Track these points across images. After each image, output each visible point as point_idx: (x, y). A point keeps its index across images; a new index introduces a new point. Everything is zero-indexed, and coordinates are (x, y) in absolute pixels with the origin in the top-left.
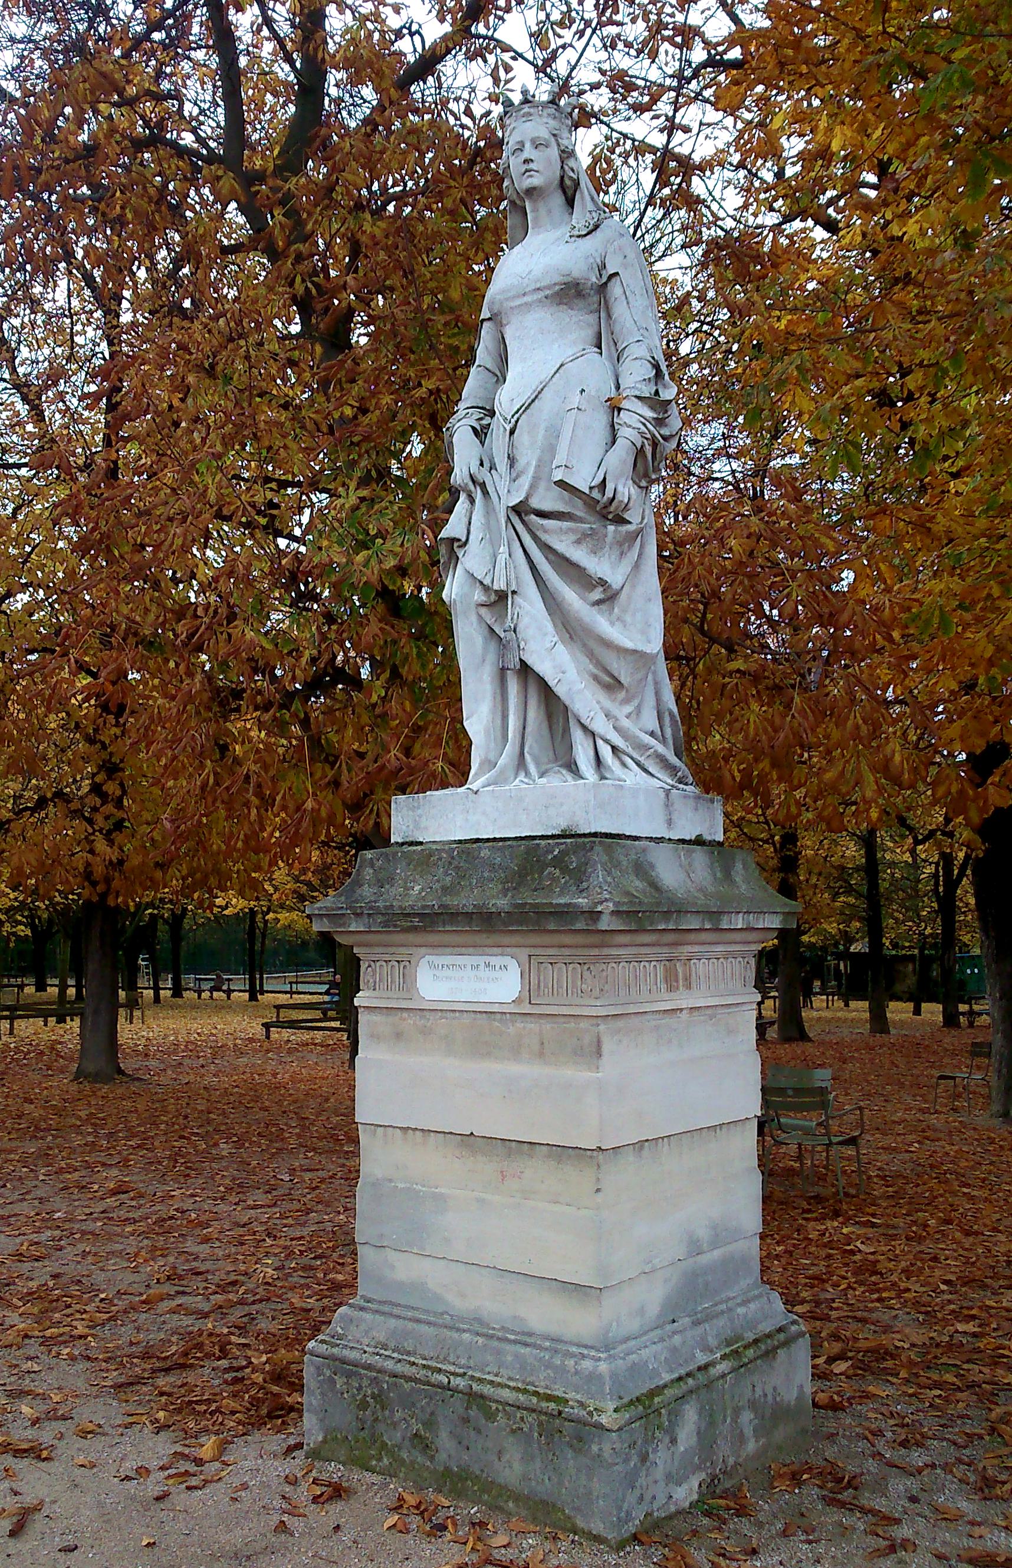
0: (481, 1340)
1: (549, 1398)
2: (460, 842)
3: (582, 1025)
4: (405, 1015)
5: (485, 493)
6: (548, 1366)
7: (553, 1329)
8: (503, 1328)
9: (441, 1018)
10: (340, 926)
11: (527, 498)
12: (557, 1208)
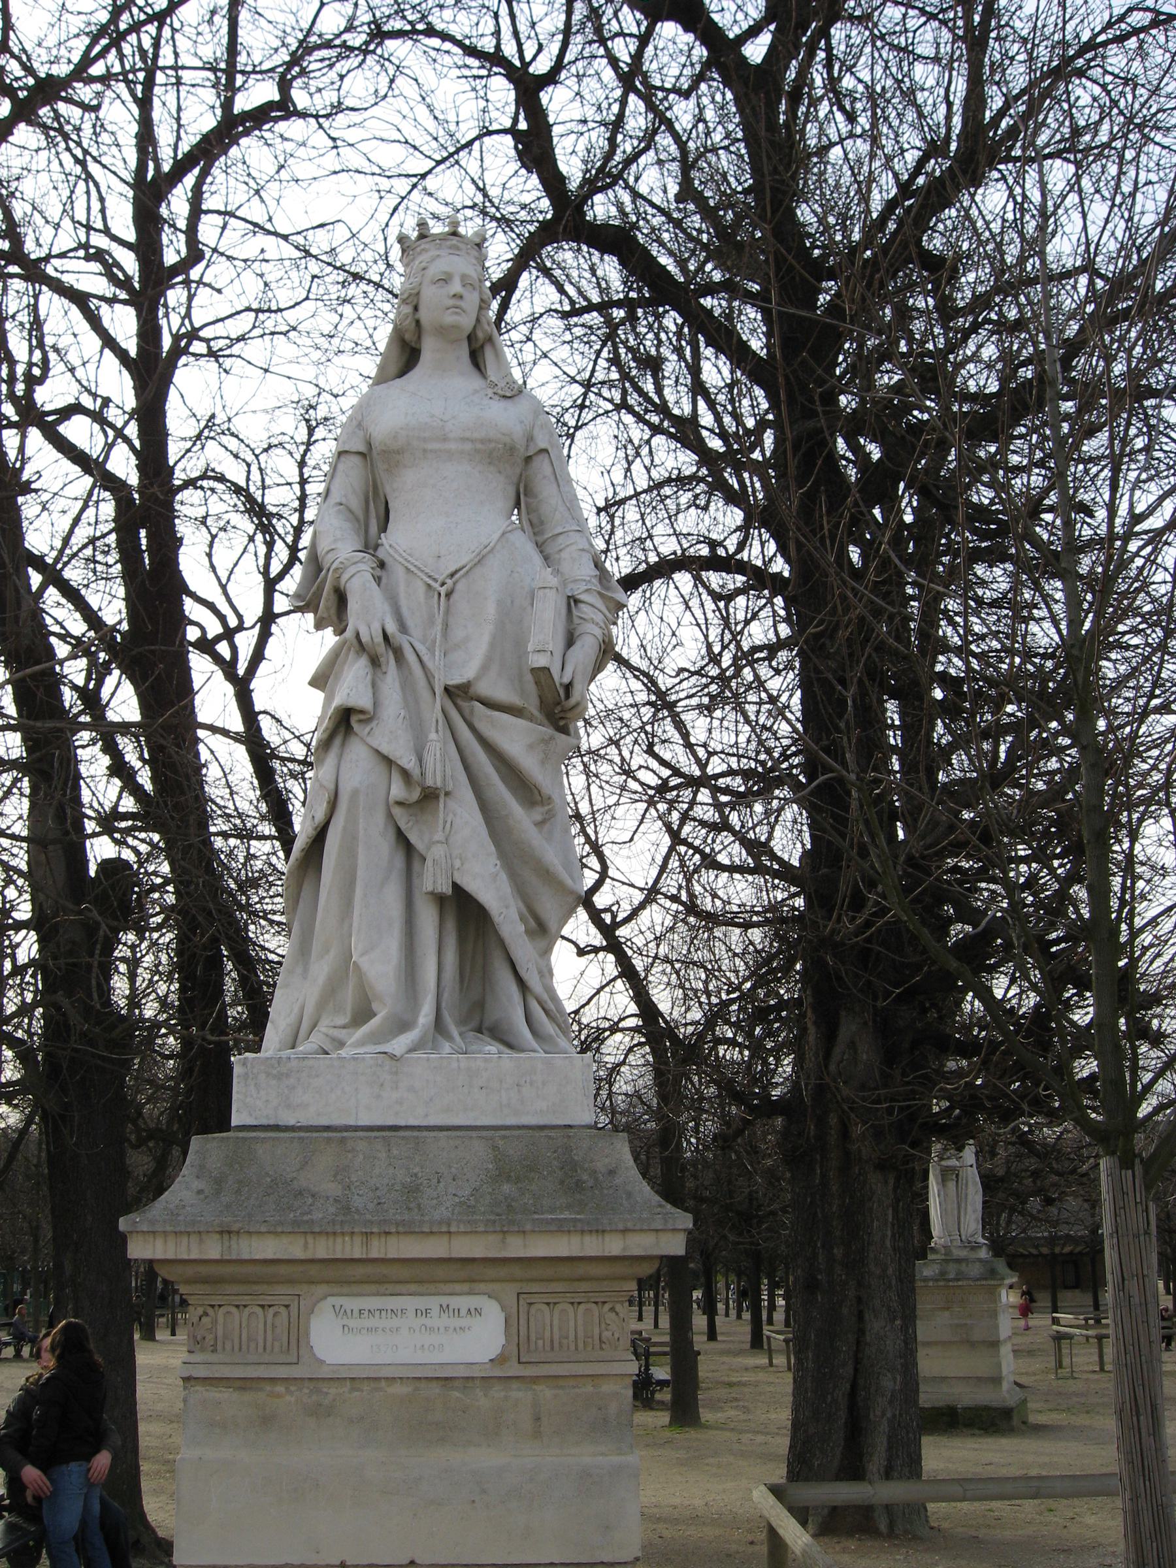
4: (280, 1389)
11: (478, 678)
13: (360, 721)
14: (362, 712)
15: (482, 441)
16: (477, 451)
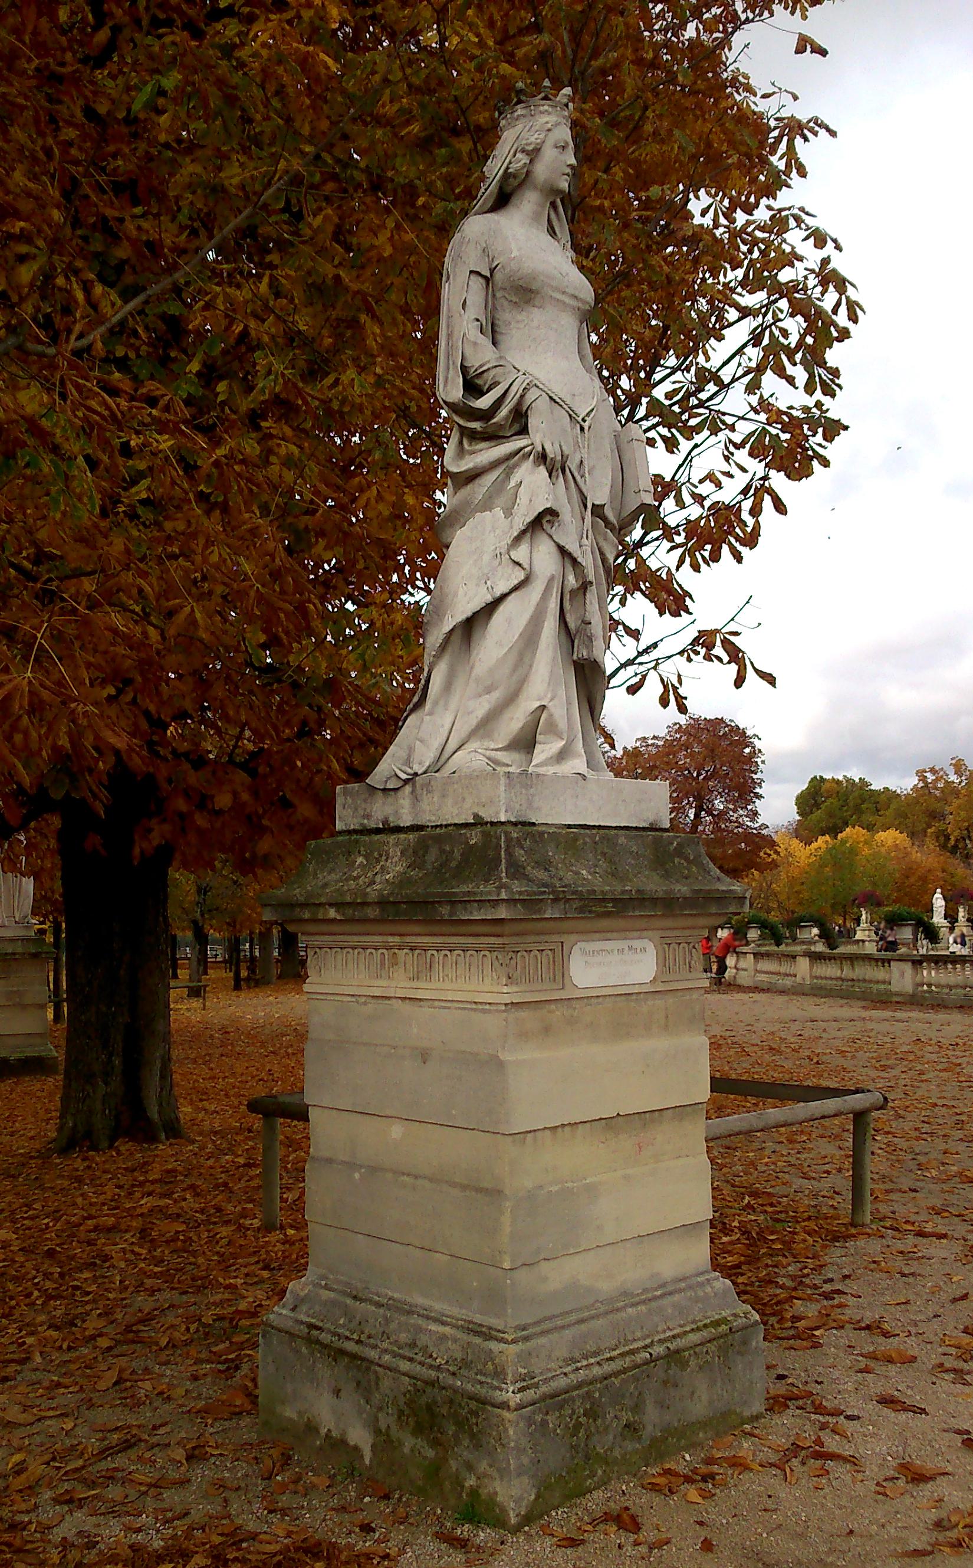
0: (643, 1308)
1: (717, 1323)
2: (569, 826)
4: (553, 1007)
6: (697, 1300)
12: (681, 1161)
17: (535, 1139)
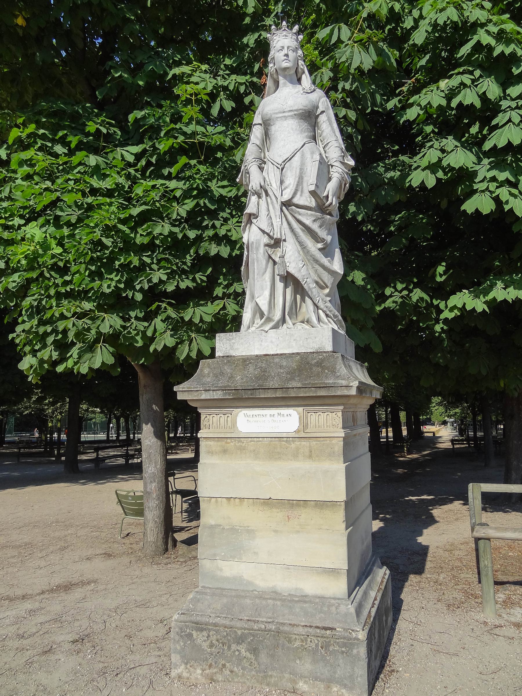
3: (333, 442)
4: (229, 440)
5: (267, 194)
7: (320, 592)
8: (290, 595)
9: (251, 441)
10: (195, 396)
11: (293, 197)
13: (254, 218)
14: (254, 215)
15: (296, 110)
16: (295, 115)
17: (217, 502)
